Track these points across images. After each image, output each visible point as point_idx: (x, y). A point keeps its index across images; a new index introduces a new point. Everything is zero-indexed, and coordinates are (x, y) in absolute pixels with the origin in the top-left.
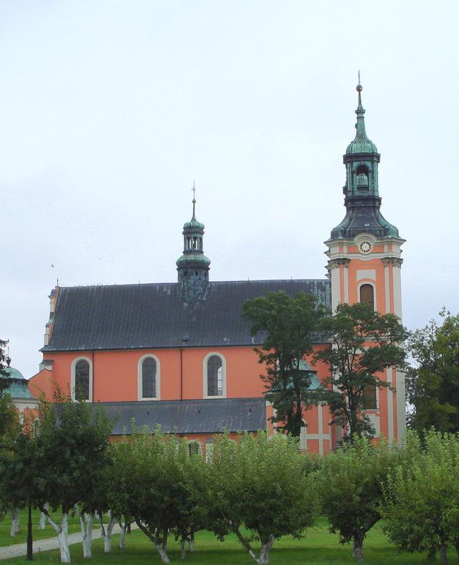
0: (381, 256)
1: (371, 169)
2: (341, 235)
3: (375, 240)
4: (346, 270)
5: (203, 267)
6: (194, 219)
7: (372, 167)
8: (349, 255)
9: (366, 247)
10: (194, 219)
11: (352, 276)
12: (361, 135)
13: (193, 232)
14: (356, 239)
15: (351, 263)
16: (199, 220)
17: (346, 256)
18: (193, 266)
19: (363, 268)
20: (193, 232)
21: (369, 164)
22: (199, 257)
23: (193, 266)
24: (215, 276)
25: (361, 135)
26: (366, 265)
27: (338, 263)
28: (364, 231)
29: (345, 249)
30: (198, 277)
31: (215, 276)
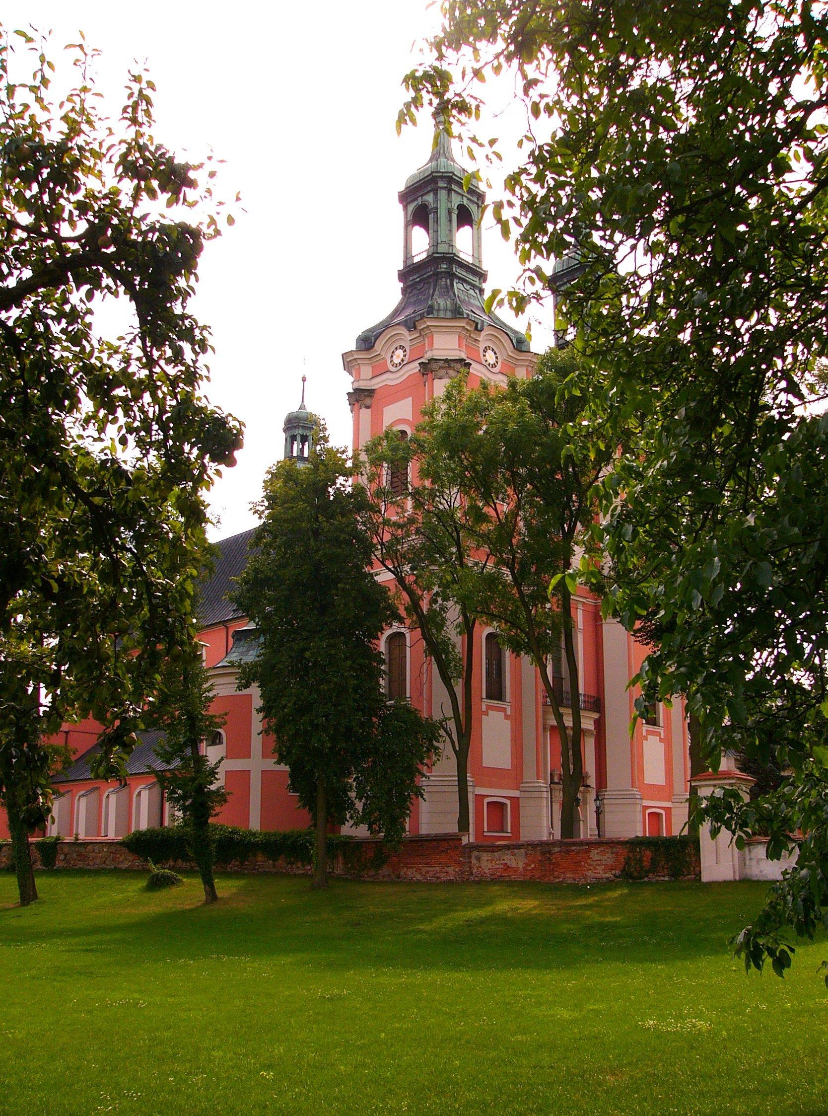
4: (365, 414)
7: (436, 200)
11: (377, 419)
14: (379, 345)
15: (377, 395)
16: (311, 408)
17: (363, 385)
21: (430, 198)
26: (395, 394)
29: (366, 371)
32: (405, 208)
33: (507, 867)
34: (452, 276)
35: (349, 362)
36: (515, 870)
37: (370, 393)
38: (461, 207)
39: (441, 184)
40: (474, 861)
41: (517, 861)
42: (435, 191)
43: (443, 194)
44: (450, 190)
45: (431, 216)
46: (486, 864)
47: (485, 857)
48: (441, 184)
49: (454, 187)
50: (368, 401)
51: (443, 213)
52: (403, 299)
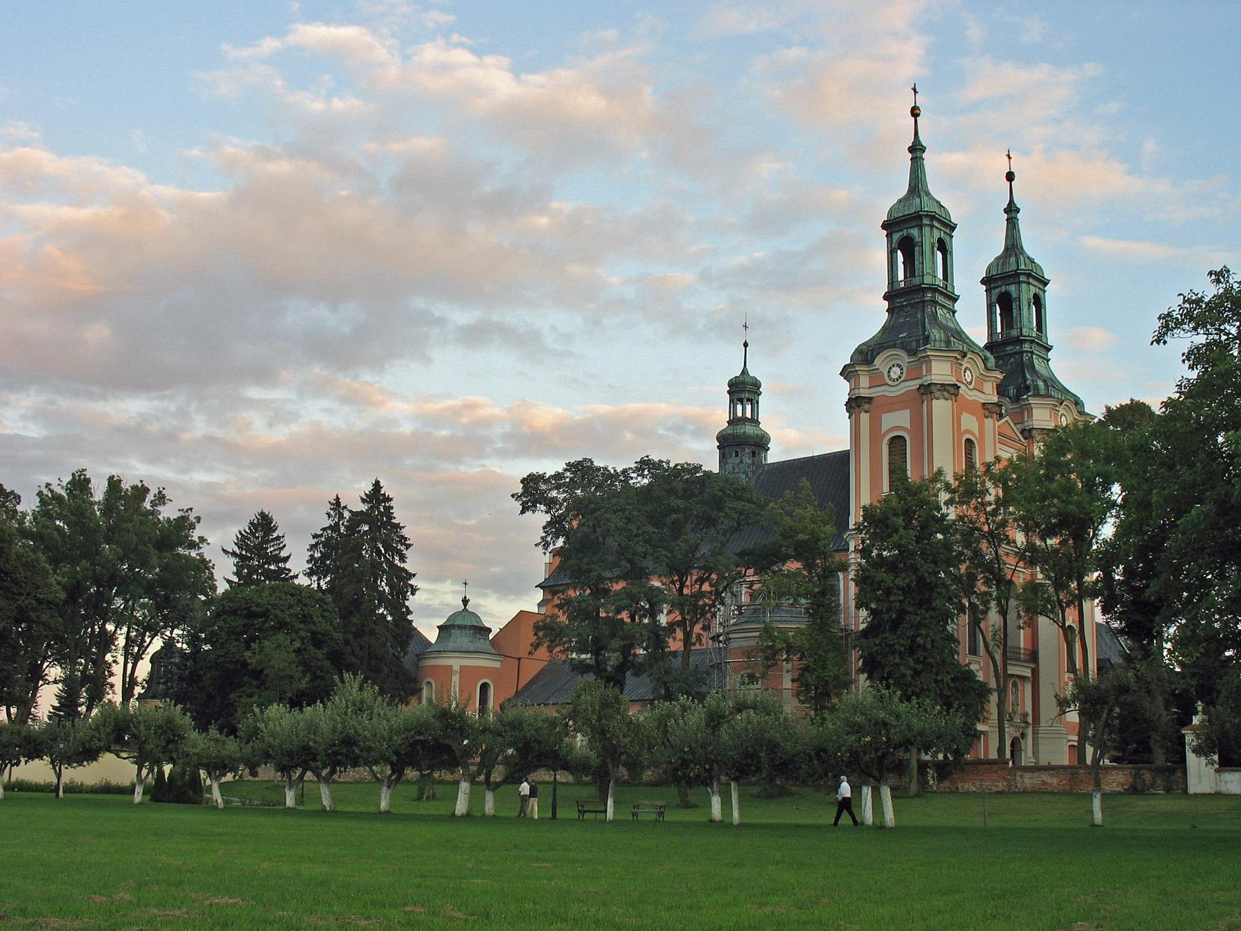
0: (918, 382)
1: (918, 239)
2: (865, 355)
3: (905, 358)
5: (761, 443)
6: (744, 372)
8: (872, 390)
9: (896, 372)
10: (744, 372)
12: (917, 184)
13: (743, 389)
14: (877, 361)
17: (864, 392)
18: (741, 441)
19: (890, 411)
20: (743, 389)
21: (915, 232)
22: (749, 429)
23: (741, 441)
24: (775, 455)
25: (917, 184)
27: (854, 404)
28: (894, 346)
29: (864, 381)
30: (737, 460)
31: (775, 455)
32: (889, 236)
33: (1044, 783)
34: (935, 303)
35: (846, 373)
36: (1051, 785)
37: (870, 400)
38: (940, 241)
39: (926, 221)
40: (1018, 778)
41: (1052, 780)
42: (921, 227)
43: (926, 230)
44: (932, 226)
45: (917, 249)
46: (1028, 780)
47: (1027, 775)
48: (926, 221)
49: (935, 223)
50: (866, 406)
51: (927, 248)
52: (889, 321)
